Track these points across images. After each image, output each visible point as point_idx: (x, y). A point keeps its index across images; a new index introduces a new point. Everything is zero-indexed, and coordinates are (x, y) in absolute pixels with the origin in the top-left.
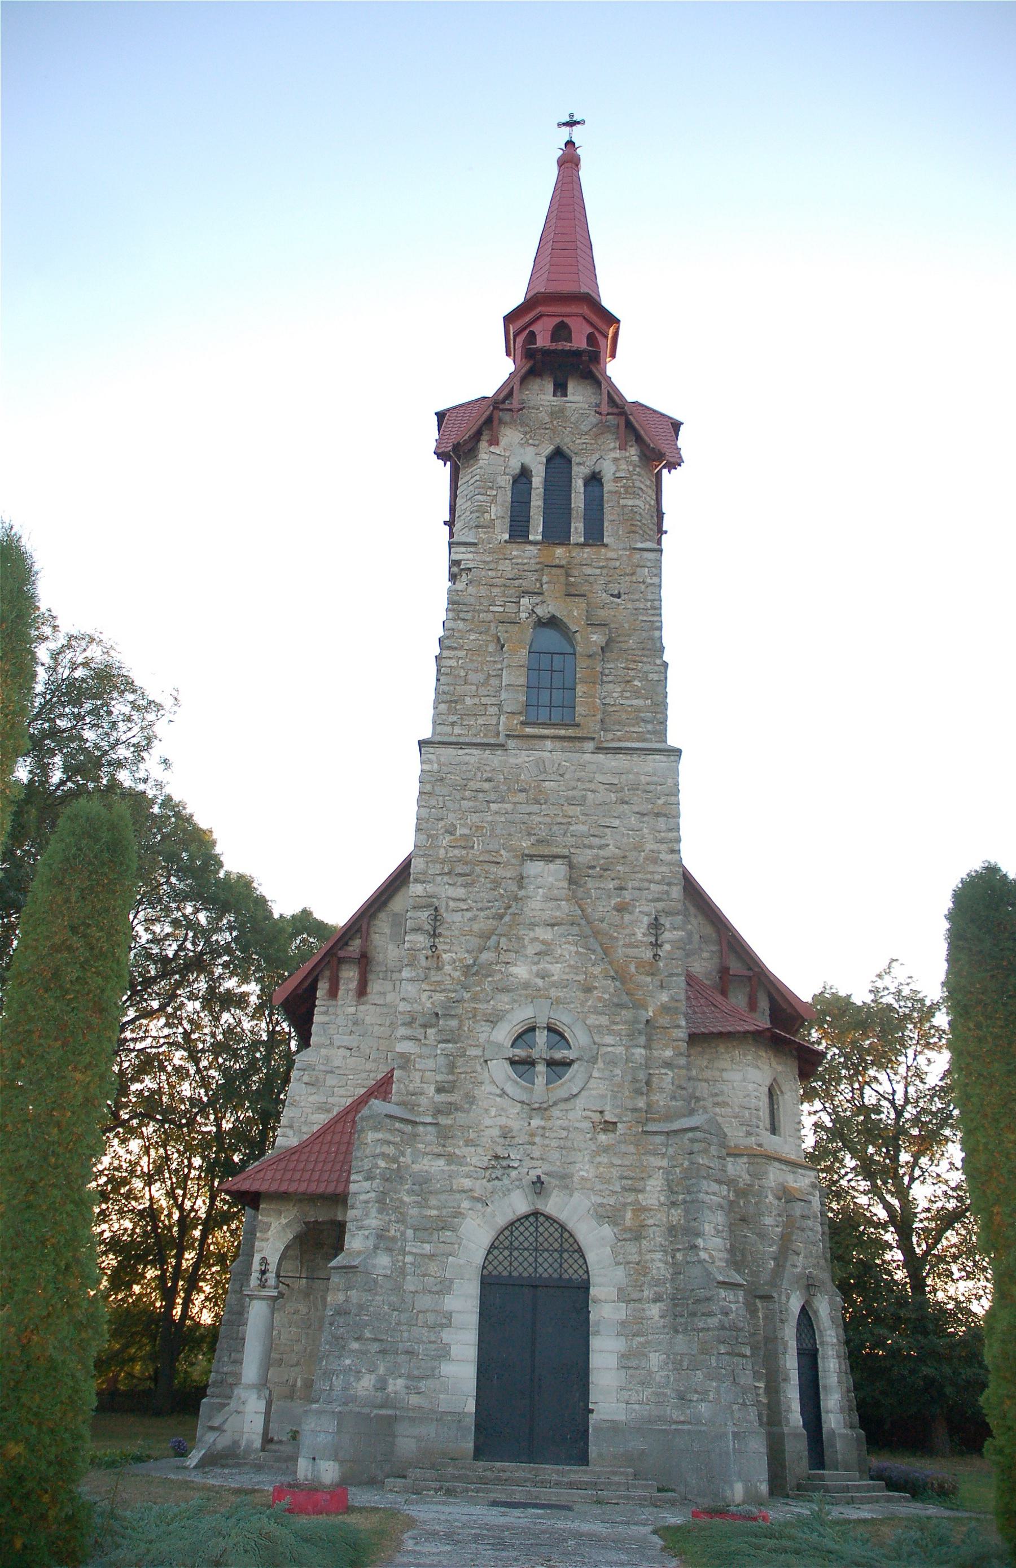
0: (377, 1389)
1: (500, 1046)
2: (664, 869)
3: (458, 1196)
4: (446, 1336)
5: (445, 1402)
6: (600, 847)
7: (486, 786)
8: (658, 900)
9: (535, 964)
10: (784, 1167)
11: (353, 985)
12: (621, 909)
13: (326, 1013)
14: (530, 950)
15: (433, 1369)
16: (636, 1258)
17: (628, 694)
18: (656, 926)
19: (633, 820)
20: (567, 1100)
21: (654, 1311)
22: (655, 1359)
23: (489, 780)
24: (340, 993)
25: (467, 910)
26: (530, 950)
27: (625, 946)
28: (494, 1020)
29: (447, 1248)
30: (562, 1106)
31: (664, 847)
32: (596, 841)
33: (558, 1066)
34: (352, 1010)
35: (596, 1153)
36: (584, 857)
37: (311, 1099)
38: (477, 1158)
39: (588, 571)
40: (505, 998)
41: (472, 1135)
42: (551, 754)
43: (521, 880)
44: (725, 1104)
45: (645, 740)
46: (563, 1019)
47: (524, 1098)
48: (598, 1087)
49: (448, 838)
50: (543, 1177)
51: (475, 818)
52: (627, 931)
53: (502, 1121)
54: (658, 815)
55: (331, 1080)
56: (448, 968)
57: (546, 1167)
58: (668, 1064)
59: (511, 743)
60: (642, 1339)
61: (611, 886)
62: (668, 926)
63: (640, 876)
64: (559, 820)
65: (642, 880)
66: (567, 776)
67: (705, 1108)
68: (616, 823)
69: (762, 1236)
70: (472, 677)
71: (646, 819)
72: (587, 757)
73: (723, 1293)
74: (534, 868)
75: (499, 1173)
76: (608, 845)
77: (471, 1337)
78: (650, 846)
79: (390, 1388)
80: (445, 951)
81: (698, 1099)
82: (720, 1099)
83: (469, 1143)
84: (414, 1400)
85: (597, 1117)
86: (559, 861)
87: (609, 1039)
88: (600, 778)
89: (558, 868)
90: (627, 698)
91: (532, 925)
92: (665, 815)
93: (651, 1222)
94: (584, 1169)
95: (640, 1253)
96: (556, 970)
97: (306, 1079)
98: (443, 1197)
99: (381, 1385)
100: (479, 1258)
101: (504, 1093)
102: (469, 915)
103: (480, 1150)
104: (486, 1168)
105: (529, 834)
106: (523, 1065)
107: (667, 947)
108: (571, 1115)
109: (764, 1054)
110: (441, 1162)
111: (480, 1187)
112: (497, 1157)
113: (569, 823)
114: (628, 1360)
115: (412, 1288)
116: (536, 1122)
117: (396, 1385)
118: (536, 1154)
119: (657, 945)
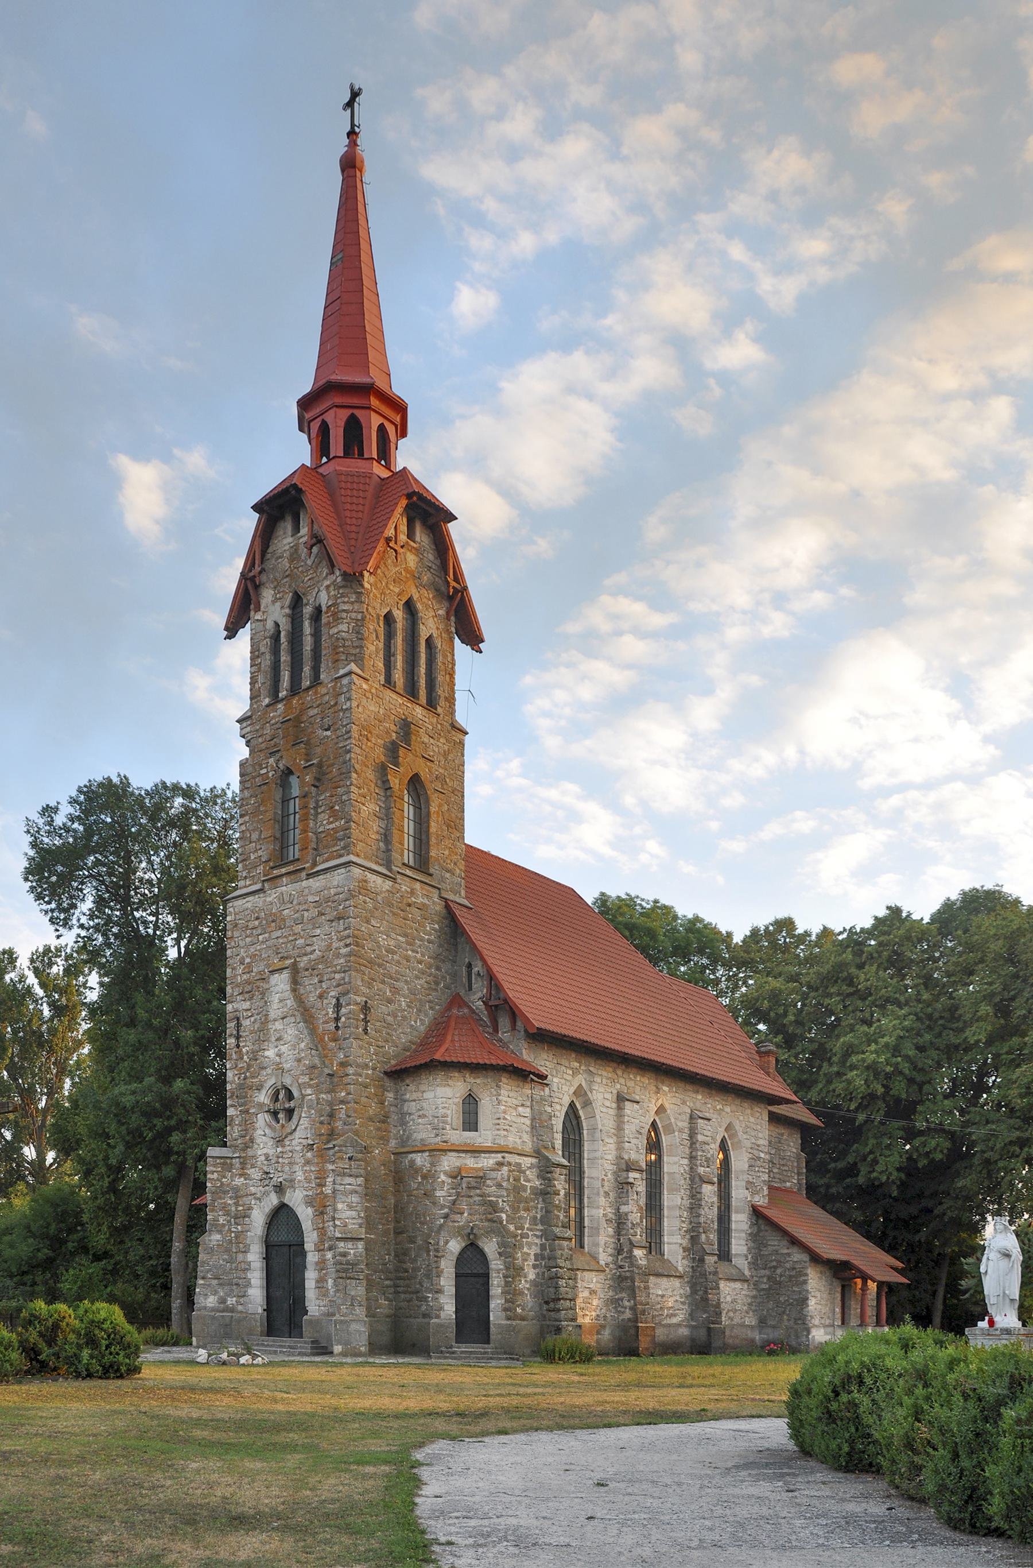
0: (220, 1303)
1: (261, 1105)
2: (342, 961)
3: (250, 1198)
4: (249, 1275)
5: (251, 1309)
6: (312, 952)
7: (257, 923)
8: (338, 985)
9: (277, 1047)
10: (463, 1155)
12: (321, 997)
14: (273, 1039)
15: (245, 1292)
16: (321, 1226)
17: (331, 819)
18: (338, 1006)
19: (327, 928)
20: (291, 1133)
21: (329, 1255)
22: (330, 1282)
23: (257, 918)
25: (251, 1016)
26: (273, 1039)
27: (324, 1023)
28: (259, 1089)
29: (247, 1229)
30: (290, 1138)
31: (342, 944)
32: (309, 949)
33: (290, 1113)
35: (305, 1165)
36: (304, 961)
38: (255, 1174)
42: (287, 888)
44: (424, 1116)
45: (341, 856)
46: (288, 1081)
47: (272, 1136)
48: (304, 1122)
49: (242, 967)
50: (284, 1182)
52: (324, 1012)
53: (265, 1151)
54: (339, 919)
56: (245, 1057)
57: (285, 1176)
58: (342, 1102)
60: (324, 1272)
61: (316, 981)
62: (344, 1003)
63: (329, 969)
64: (291, 938)
65: (331, 972)
66: (295, 902)
67: (413, 1120)
68: (318, 931)
69: (434, 1203)
71: (333, 924)
72: (304, 883)
73: (342, 1244)
75: (267, 1182)
76: (315, 950)
78: (335, 945)
79: (229, 1303)
80: (244, 1047)
81: (410, 1114)
82: (421, 1113)
83: (253, 1166)
84: (240, 1308)
85: (305, 1142)
86: (285, 971)
87: (309, 1091)
88: (311, 899)
89: (285, 975)
90: (332, 823)
91: (275, 1020)
92: (343, 918)
93: (328, 1203)
94: (300, 1176)
95: (323, 1222)
96: (284, 1049)
98: (244, 1199)
99: (223, 1301)
102: (252, 1019)
103: (257, 1169)
104: (261, 1180)
105: (277, 953)
106: (275, 1114)
107: (343, 1019)
108: (294, 1143)
109: (456, 1074)
110: (242, 1179)
112: (267, 1173)
113: (296, 939)
114: (321, 1281)
115: (234, 1250)
116: (279, 1149)
117: (231, 1301)
118: (279, 1169)
119: (337, 1019)
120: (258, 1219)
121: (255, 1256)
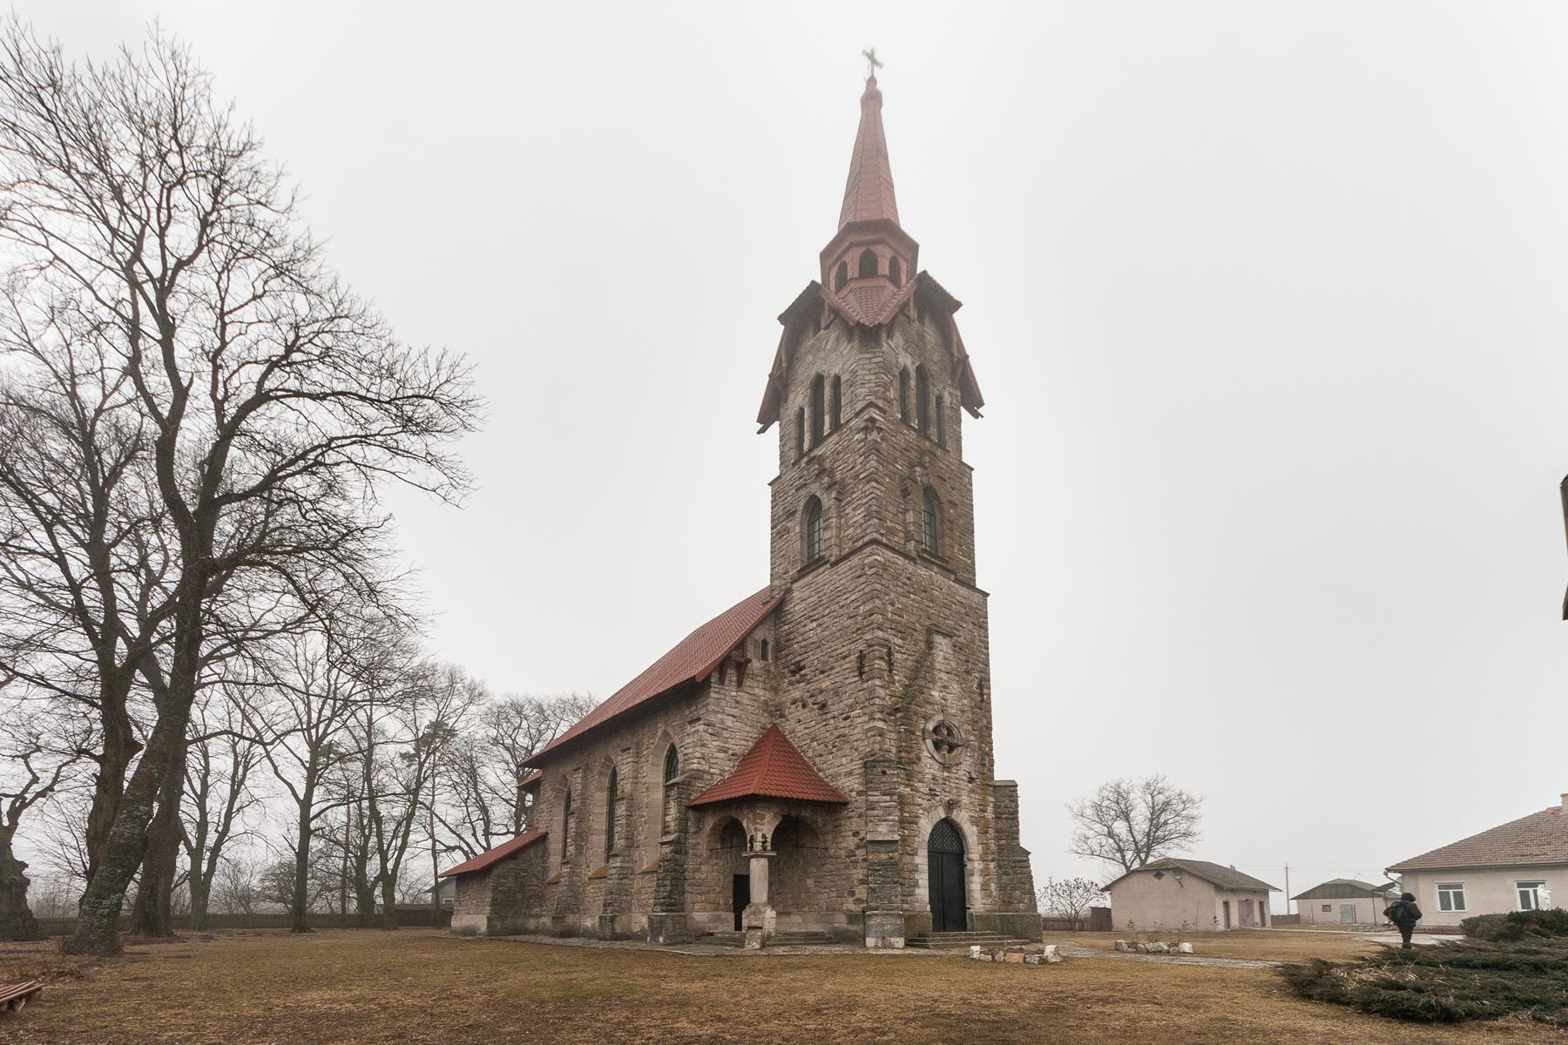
11: (734, 679)
13: (716, 692)
14: (939, 684)
23: (909, 579)
24: (727, 682)
34: (735, 694)
37: (714, 743)
39: (941, 465)
40: (930, 707)
41: (920, 776)
43: (930, 645)
51: (903, 600)
53: (932, 771)
55: (726, 734)
59: (919, 561)
70: (890, 508)
74: (938, 639)
77: (925, 876)
97: (710, 731)
100: (927, 839)
101: (933, 757)
102: (905, 656)
106: (937, 745)
111: (925, 804)
120: (926, 826)
121: (922, 860)
